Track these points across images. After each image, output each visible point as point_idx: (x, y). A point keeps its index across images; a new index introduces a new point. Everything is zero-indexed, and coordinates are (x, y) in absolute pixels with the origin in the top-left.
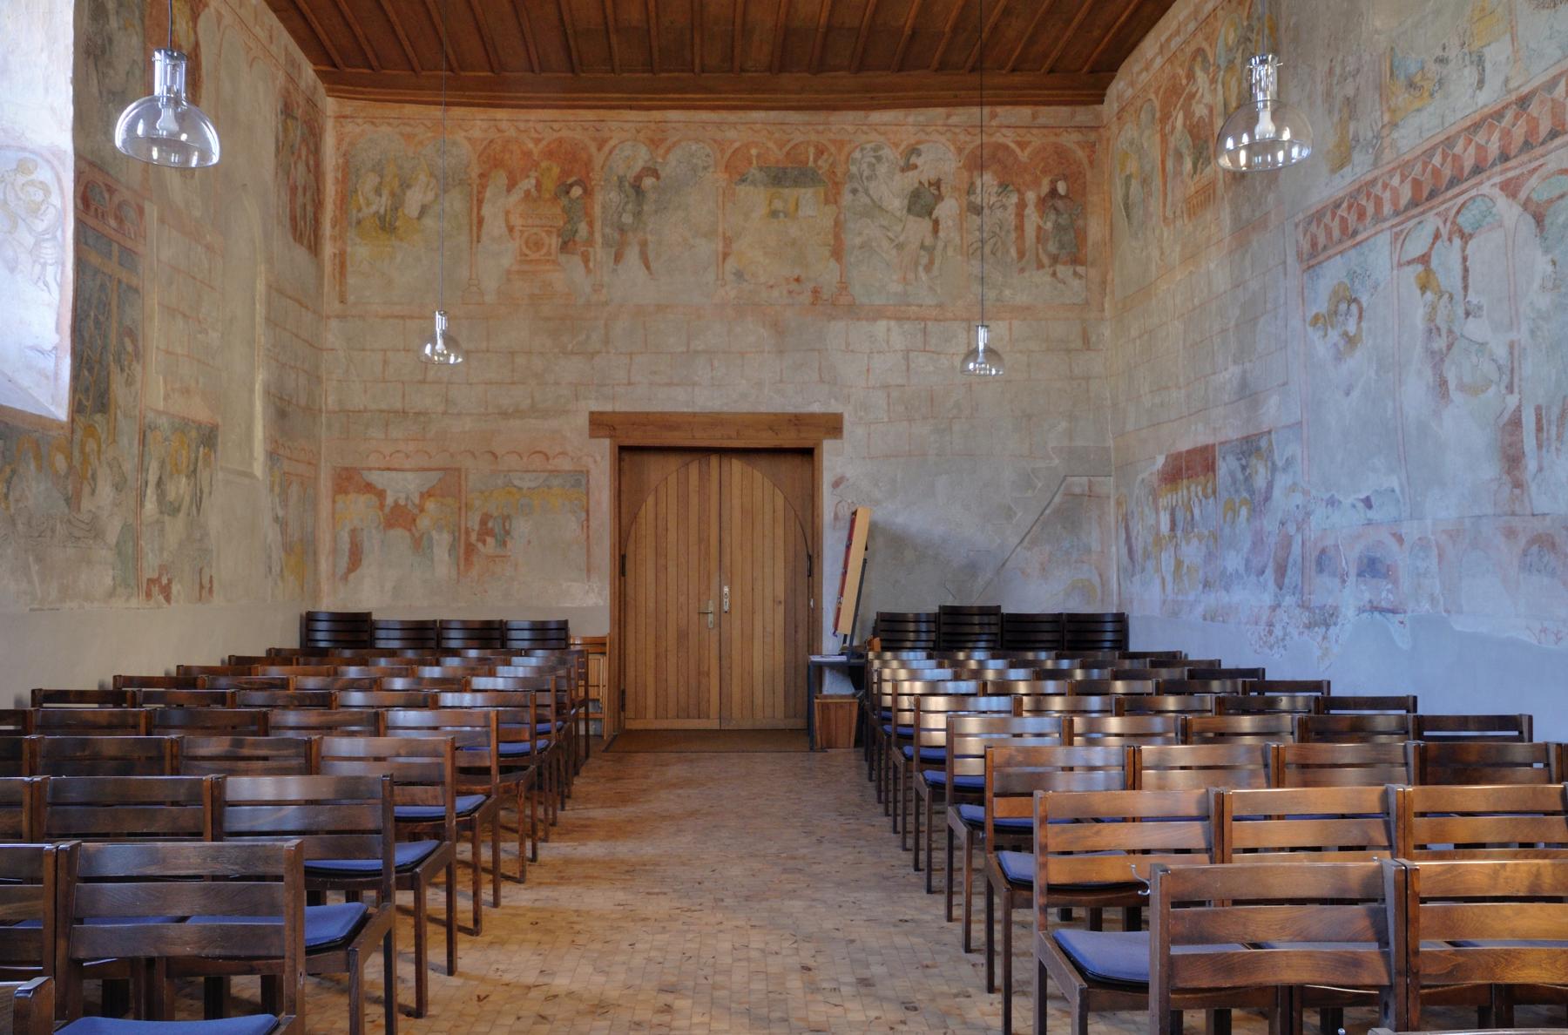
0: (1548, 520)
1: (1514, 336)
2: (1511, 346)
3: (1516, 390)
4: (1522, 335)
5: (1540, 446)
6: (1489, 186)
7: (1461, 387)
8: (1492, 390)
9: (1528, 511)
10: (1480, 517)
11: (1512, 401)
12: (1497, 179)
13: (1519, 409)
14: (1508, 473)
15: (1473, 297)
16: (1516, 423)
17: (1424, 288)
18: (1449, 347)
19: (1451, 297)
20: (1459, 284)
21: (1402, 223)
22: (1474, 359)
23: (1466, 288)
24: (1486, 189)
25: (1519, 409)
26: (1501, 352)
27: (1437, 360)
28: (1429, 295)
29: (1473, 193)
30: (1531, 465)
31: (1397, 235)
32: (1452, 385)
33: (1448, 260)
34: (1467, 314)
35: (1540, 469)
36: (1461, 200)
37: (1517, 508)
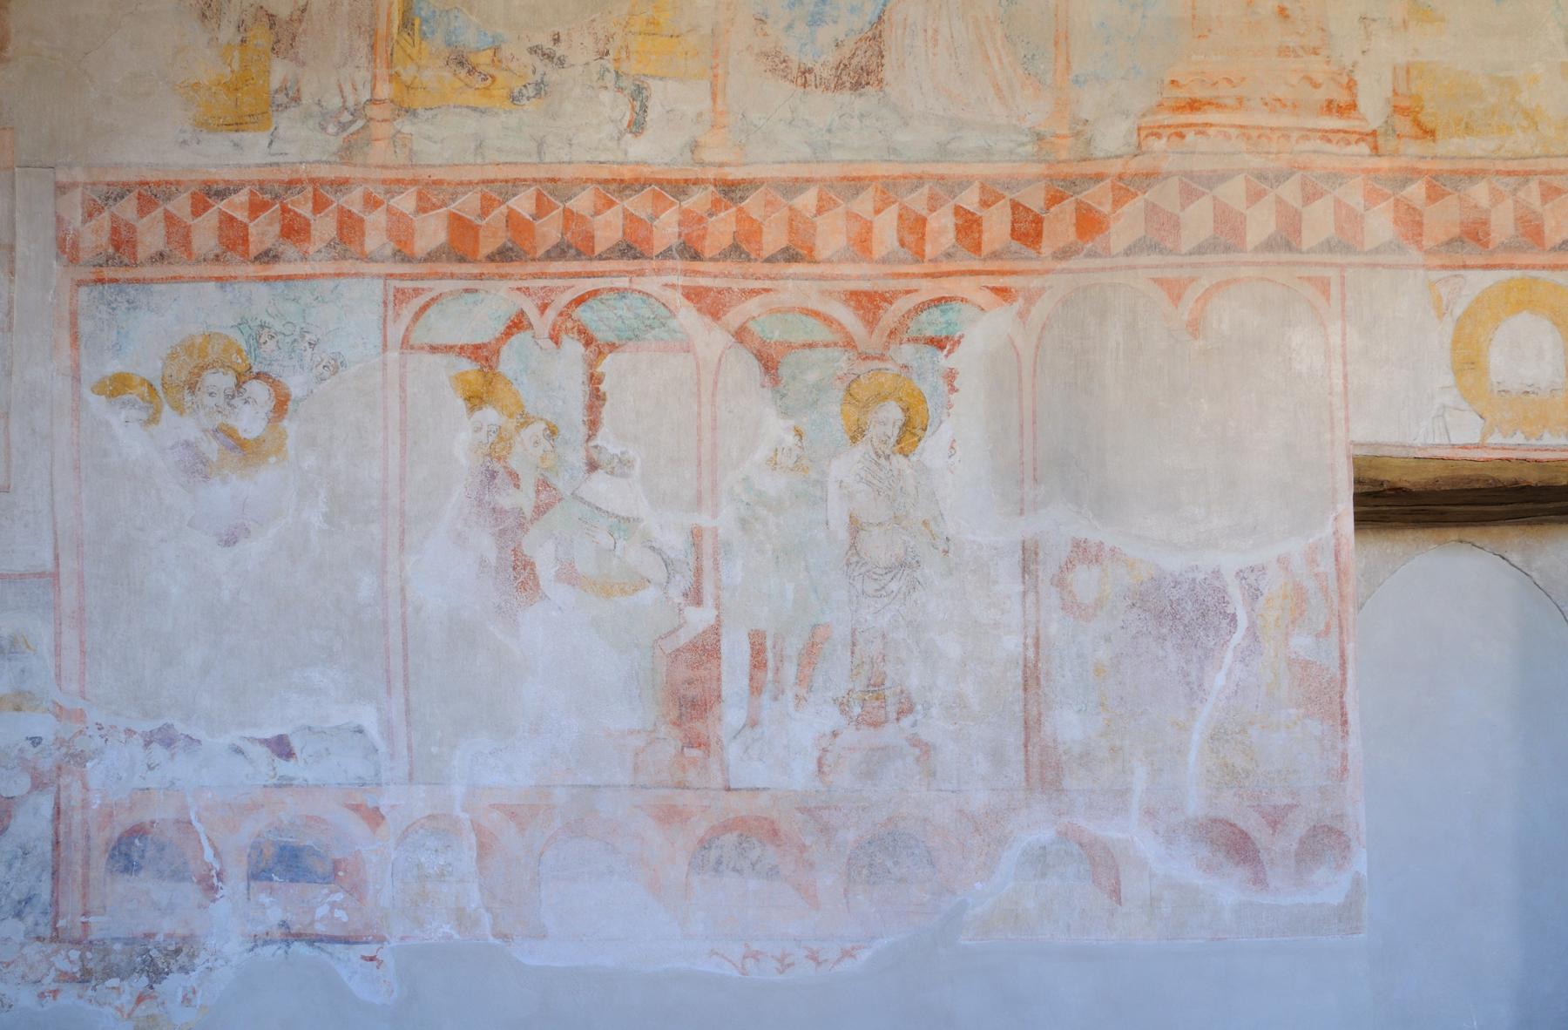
0: (763, 799)
1: (704, 520)
2: (696, 535)
3: (708, 600)
4: (724, 521)
5: (756, 688)
6: (661, 282)
7: (569, 575)
8: (649, 595)
9: (718, 782)
10: (594, 787)
11: (699, 618)
12: (680, 281)
13: (716, 630)
14: (677, 723)
15: (607, 441)
16: (707, 649)
17: (475, 400)
18: (541, 510)
19: (552, 432)
20: (578, 415)
21: (421, 277)
22: (606, 540)
23: (593, 424)
24: (651, 284)
25: (716, 630)
26: (675, 542)
27: (510, 528)
28: (490, 415)
29: (622, 282)
30: (732, 714)
31: (401, 297)
32: (546, 571)
33: (548, 374)
34: (593, 466)
35: (753, 723)
36: (588, 285)
37: (692, 776)
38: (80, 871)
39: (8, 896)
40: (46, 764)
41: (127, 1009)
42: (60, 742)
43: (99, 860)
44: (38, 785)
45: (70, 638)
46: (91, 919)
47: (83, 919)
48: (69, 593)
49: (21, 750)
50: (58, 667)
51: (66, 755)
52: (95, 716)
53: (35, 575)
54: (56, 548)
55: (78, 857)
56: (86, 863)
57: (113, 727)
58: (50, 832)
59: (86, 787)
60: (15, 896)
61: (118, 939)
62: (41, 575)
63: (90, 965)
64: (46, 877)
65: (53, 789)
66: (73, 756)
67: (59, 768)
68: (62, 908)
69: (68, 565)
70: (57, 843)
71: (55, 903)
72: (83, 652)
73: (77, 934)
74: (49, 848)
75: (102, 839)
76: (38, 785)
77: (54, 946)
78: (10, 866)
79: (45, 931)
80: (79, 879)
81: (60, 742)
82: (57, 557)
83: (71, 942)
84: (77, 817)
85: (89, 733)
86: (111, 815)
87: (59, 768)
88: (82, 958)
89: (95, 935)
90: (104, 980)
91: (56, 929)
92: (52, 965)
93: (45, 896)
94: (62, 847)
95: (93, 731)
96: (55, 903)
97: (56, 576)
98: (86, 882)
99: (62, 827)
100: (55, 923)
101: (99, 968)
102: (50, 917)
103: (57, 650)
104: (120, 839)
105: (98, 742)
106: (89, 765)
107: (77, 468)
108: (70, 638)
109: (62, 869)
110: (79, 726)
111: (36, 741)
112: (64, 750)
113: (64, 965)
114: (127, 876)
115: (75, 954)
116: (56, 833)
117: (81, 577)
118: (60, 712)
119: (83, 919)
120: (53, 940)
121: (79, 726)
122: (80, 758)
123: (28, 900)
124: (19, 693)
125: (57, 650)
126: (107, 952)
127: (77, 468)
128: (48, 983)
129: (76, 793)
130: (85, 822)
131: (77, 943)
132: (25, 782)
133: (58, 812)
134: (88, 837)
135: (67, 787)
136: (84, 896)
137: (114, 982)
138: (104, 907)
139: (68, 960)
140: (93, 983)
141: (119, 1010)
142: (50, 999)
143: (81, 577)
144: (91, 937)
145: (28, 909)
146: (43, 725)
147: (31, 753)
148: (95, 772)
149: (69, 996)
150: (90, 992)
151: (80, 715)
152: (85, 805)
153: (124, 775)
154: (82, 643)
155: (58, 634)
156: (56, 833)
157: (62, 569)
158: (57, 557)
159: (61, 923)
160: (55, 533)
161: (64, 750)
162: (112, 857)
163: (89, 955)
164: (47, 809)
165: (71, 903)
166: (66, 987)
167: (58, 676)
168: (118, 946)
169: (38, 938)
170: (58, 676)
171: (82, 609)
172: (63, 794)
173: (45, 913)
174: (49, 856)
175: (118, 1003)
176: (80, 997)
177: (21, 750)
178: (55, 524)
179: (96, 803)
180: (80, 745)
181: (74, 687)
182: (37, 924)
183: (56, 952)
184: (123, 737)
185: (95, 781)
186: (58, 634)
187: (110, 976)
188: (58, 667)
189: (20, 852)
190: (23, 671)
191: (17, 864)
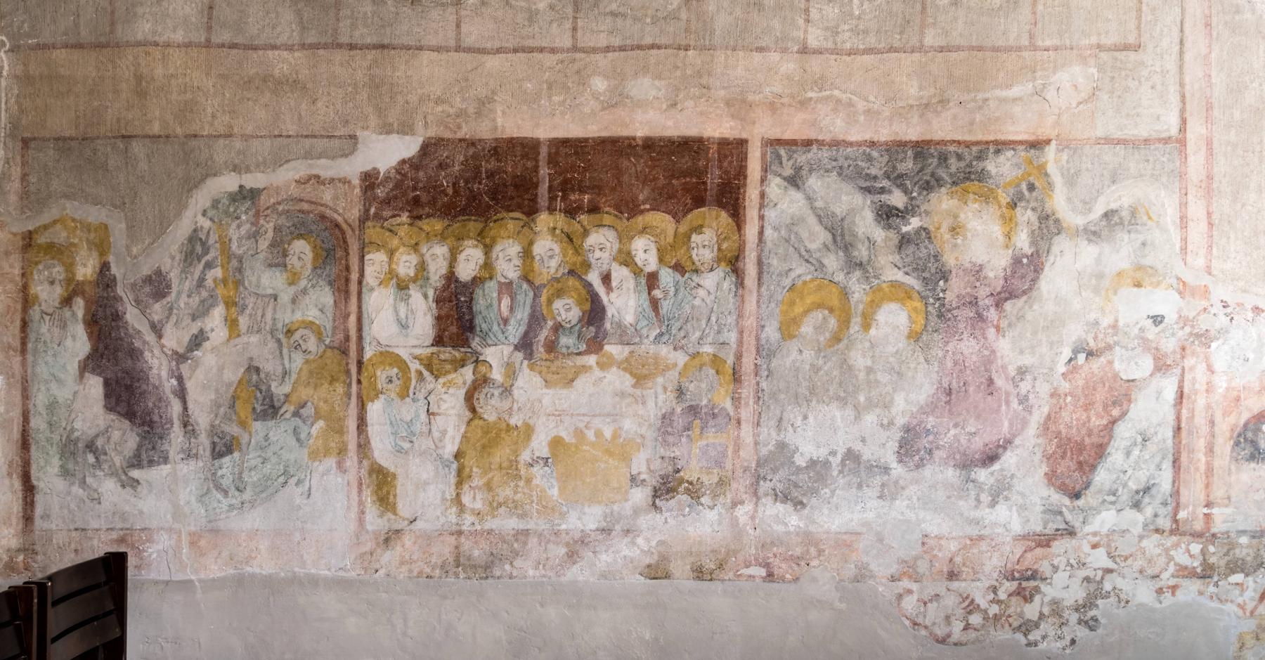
38: (1203, 459)
39: (1125, 485)
40: (1169, 346)
41: (1249, 607)
42: (1184, 321)
43: (1224, 447)
44: (1161, 366)
45: (1196, 209)
46: (1215, 511)
47: (1206, 511)
48: (1196, 161)
49: (1142, 330)
50: (1184, 240)
51: (1191, 334)
52: (1220, 292)
53: (1160, 140)
54: (1183, 111)
55: (1201, 444)
56: (1210, 450)
57: (1240, 305)
58: (1171, 418)
59: (1211, 370)
60: (1133, 486)
61: (1243, 532)
62: (1166, 141)
63: (1213, 560)
64: (1167, 465)
65: (1178, 371)
66: (1198, 336)
67: (1183, 349)
68: (1183, 500)
69: (1196, 130)
70: (1178, 429)
71: (1176, 493)
72: (1211, 224)
73: (1198, 526)
74: (1170, 434)
75: (1224, 428)
76: (1161, 366)
77: (1174, 539)
78: (1128, 454)
79: (1165, 523)
80: (1202, 467)
81: (1184, 321)
82: (1184, 121)
83: (1192, 535)
84: (1201, 402)
85: (1213, 311)
86: (1238, 399)
87: (1183, 349)
88: (1203, 552)
89: (1218, 526)
90: (1227, 576)
91: (1176, 521)
92: (1171, 559)
93: (1165, 484)
94: (1184, 433)
95: (1218, 308)
96: (1176, 493)
97: (1182, 142)
98: (1210, 471)
99: (1185, 413)
100: (1175, 514)
101: (1222, 563)
102: (1170, 508)
103: (1184, 222)
104: (1246, 425)
105: (1224, 320)
106: (1214, 345)
107: (1208, 25)
108: (1196, 209)
109: (1184, 458)
110: (1204, 303)
111: (1157, 320)
112: (1188, 329)
113: (1183, 559)
114: (1253, 465)
115: (1196, 548)
116: (1178, 419)
117: (1209, 144)
118: (1183, 289)
119: (1206, 511)
120: (1173, 532)
121: (1204, 303)
122: (1205, 338)
123: (1147, 490)
124: (1139, 268)
125: (1184, 222)
126: (1232, 546)
127: (1208, 25)
128: (1167, 578)
129: (1200, 374)
130: (1208, 407)
131: (1197, 535)
132: (1147, 364)
133: (1181, 395)
134: (1212, 423)
135: (1192, 369)
136: (1207, 486)
137: (1238, 578)
138: (1229, 498)
139: (1188, 553)
140: (1216, 579)
141: (1240, 606)
142: (1168, 595)
143: (1209, 144)
144: (1214, 530)
145: (1146, 500)
146: (1165, 302)
147: (1152, 332)
148: (1220, 354)
149: (1190, 590)
150: (1212, 589)
151: (1206, 292)
152: (1210, 389)
153: (1251, 356)
154: (1209, 214)
155: (1183, 205)
156: (1178, 419)
157: (1189, 135)
158: (1184, 121)
159: (1182, 515)
160: (1183, 97)
161: (1188, 329)
162: (1237, 444)
163: (1212, 549)
164: (1170, 394)
165: (1193, 493)
166: (1185, 583)
167: (1184, 249)
168: (1244, 540)
169: (1157, 531)
170: (1184, 249)
171: (1210, 177)
172: (1188, 377)
173: (1165, 504)
174: (1170, 442)
175: (1240, 600)
176: (1201, 593)
177: (1142, 330)
178: (1182, 85)
179: (1221, 384)
180: (1203, 324)
181: (1201, 262)
182: (1156, 516)
183: (1176, 546)
184: (1250, 315)
185: (1219, 365)
186: (1183, 205)
187: (1233, 572)
188: (1184, 240)
189: (1139, 439)
190: (1144, 244)
191: (1136, 452)
